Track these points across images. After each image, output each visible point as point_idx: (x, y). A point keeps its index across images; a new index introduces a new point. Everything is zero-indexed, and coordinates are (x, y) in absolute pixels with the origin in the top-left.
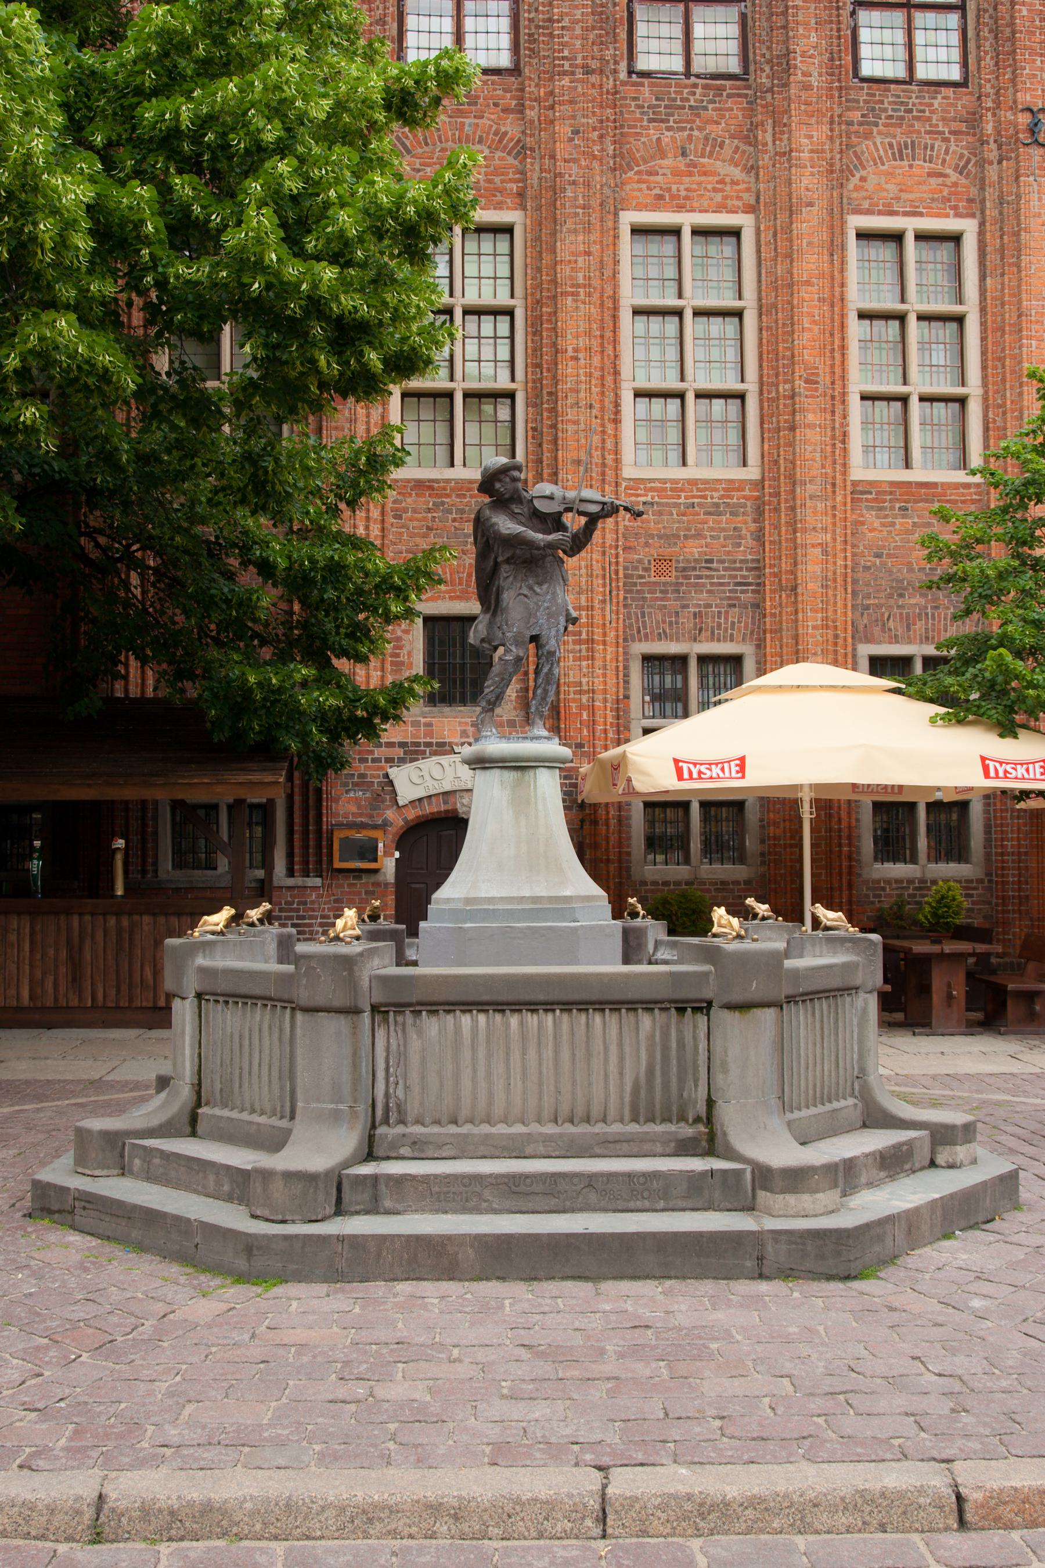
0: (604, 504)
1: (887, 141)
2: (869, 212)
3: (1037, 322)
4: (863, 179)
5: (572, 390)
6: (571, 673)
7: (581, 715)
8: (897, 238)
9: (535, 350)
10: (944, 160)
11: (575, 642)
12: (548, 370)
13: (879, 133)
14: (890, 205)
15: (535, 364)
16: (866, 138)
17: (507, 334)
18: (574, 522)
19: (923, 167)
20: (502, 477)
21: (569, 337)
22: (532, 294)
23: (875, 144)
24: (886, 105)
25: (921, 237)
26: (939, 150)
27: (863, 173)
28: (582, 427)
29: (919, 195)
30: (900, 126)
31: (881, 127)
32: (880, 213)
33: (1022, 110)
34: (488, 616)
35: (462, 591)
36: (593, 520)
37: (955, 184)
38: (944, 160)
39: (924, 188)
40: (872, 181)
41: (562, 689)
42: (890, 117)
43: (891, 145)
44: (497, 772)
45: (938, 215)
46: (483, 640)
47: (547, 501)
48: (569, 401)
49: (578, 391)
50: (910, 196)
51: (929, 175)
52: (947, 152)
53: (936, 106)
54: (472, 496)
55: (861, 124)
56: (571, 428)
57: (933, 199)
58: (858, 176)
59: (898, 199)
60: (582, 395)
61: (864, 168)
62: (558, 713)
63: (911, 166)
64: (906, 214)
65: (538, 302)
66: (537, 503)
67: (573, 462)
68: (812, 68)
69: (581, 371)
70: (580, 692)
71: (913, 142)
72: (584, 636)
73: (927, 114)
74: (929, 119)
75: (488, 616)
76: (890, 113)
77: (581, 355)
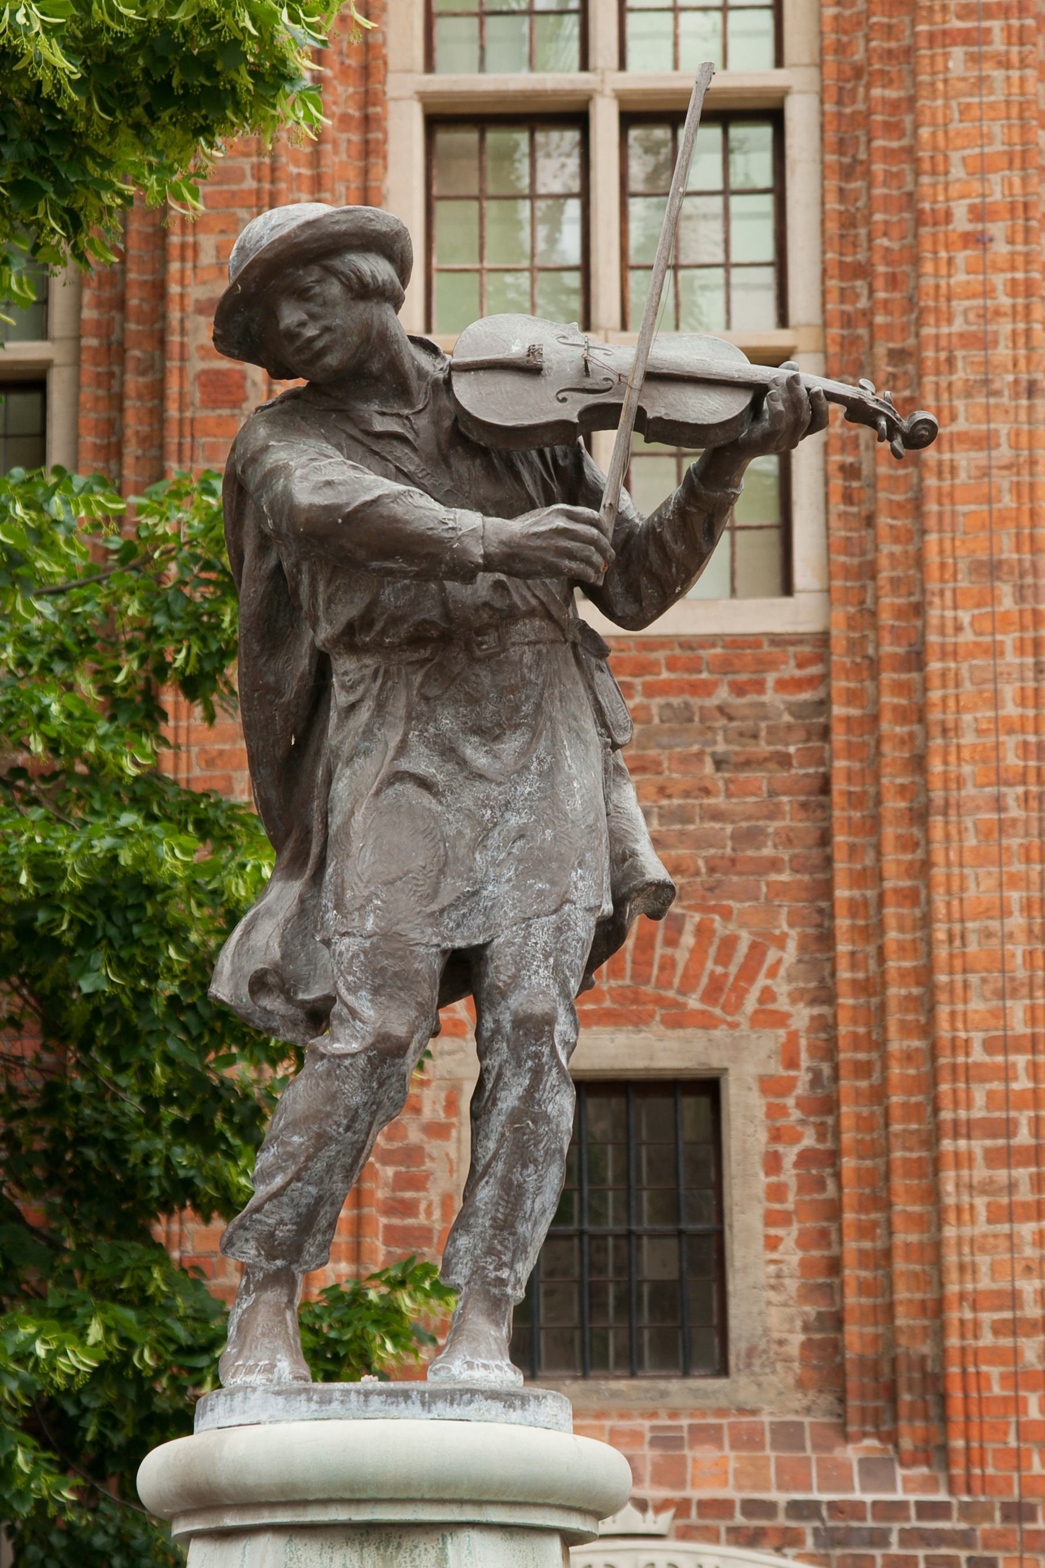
0: (759, 391)
5: (968, 340)
6: (984, 1261)
7: (1018, 1405)
9: (848, 222)
11: (993, 1158)
12: (893, 282)
15: (846, 270)
17: (764, 178)
18: (647, 486)
20: (310, 276)
21: (957, 172)
22: (840, 49)
28: (1004, 453)
34: (296, 887)
35: (620, 996)
36: (718, 458)
41: (953, 1316)
44: (266, 1546)
46: (259, 983)
47: (510, 382)
48: (961, 374)
49: (984, 342)
54: (650, 691)
56: (966, 459)
60: (1003, 352)
62: (943, 1399)
65: (858, 72)
66: (467, 392)
67: (976, 568)
69: (999, 280)
70: (1013, 1328)
72: (1024, 1137)
75: (296, 887)
77: (997, 229)
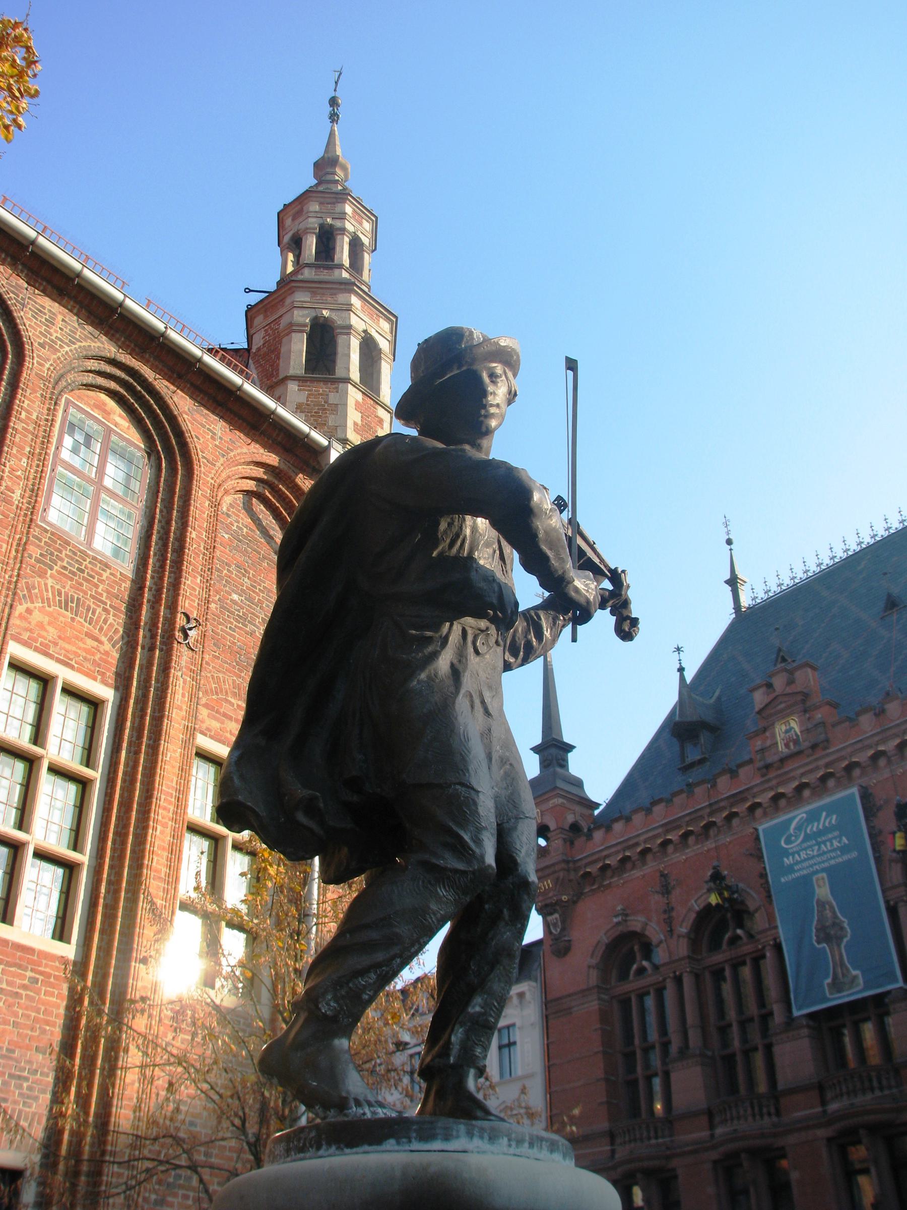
1: (57, 587)
2: (25, 644)
3: (165, 809)
4: (29, 611)
8: (45, 681)
10: (101, 629)
13: (52, 576)
14: (47, 646)
16: (40, 576)
19: (83, 626)
23: (46, 585)
24: (63, 556)
25: (70, 692)
26: (99, 617)
27: (29, 605)
29: (74, 649)
30: (72, 580)
31: (54, 572)
32: (36, 650)
33: (184, 613)
37: (107, 653)
38: (101, 629)
39: (82, 645)
40: (37, 616)
42: (65, 568)
43: (60, 594)
45: (87, 675)
50: (67, 646)
51: (87, 634)
52: (105, 621)
53: (104, 578)
55: (38, 561)
57: (85, 658)
58: (25, 606)
59: (56, 644)
61: (32, 602)
63: (73, 619)
64: (59, 661)
68: (15, 487)
71: (78, 599)
73: (96, 581)
74: (97, 586)
76: (65, 564)
